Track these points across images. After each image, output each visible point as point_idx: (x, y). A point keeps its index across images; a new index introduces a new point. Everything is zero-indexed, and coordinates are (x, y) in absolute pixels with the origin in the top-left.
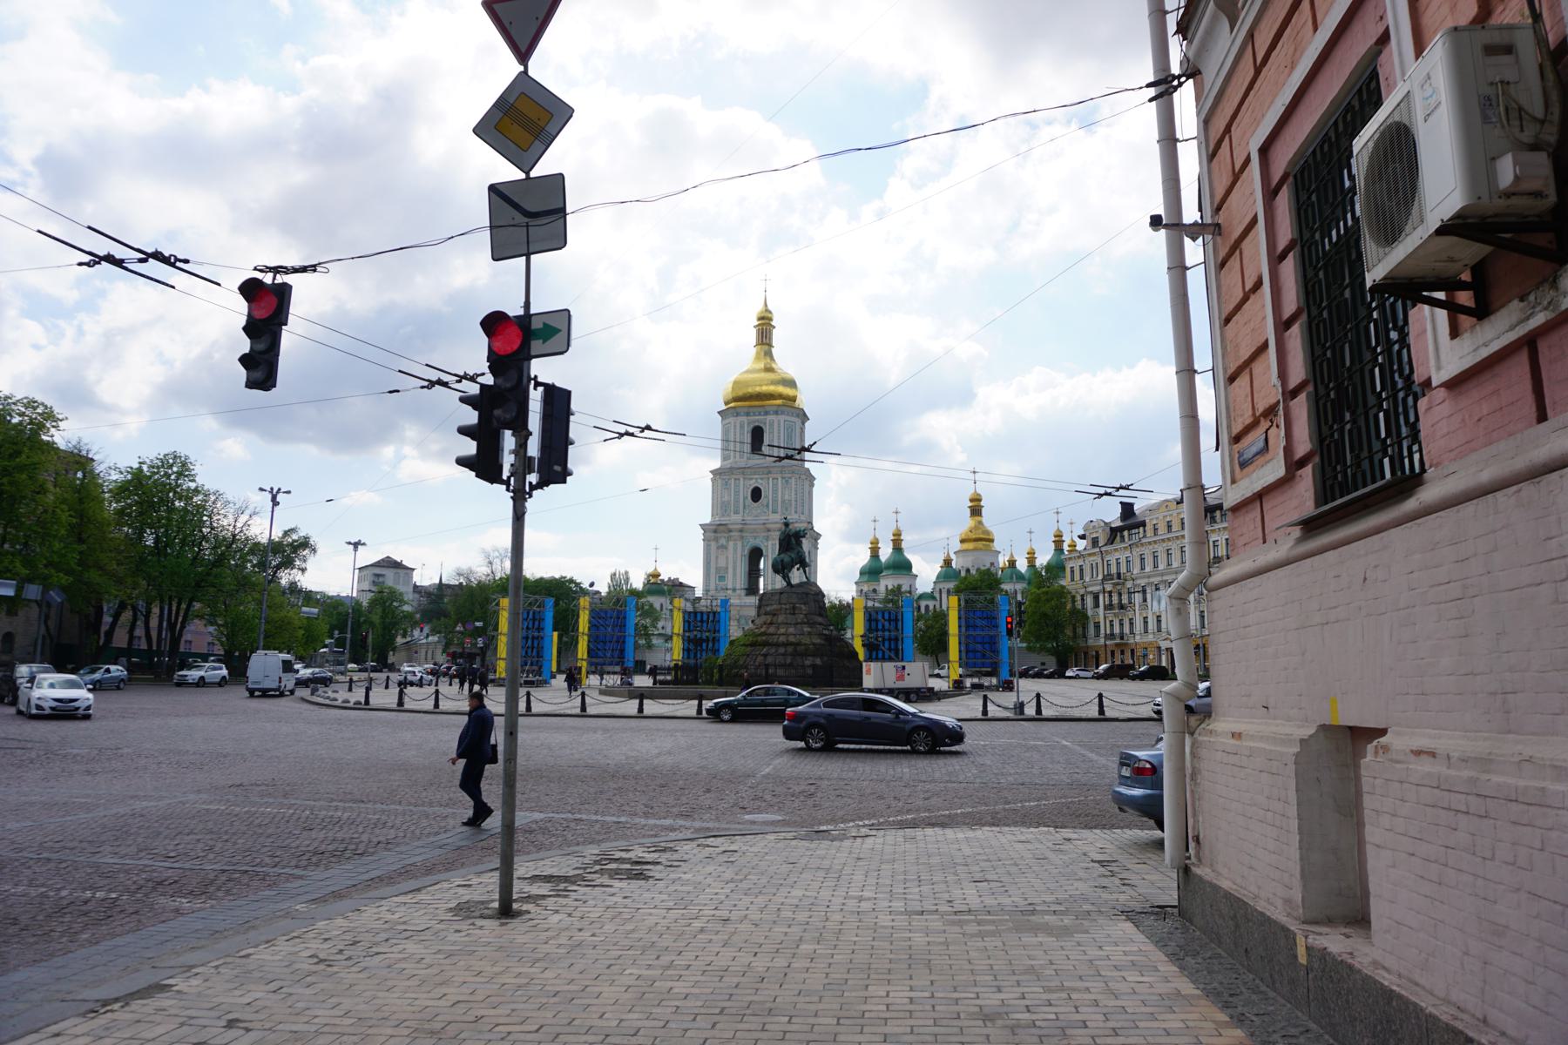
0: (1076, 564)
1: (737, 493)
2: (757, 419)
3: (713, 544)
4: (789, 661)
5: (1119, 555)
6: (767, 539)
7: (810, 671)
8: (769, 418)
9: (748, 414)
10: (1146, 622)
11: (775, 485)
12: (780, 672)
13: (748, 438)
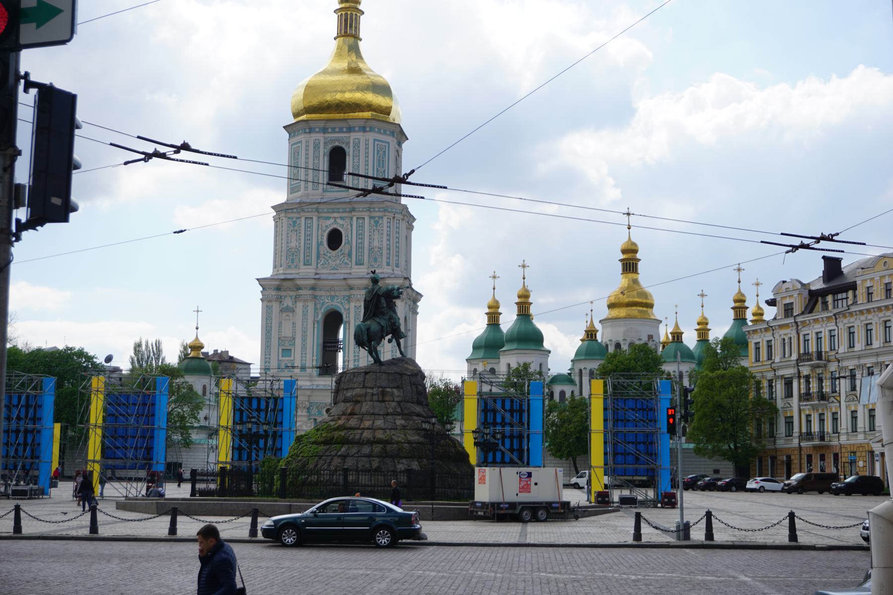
0: (762, 339)
1: (308, 237)
2: (337, 138)
3: (276, 306)
4: (375, 464)
5: (820, 328)
6: (349, 299)
7: (403, 479)
8: (353, 135)
9: (324, 130)
10: (854, 418)
11: (361, 227)
12: (364, 479)
13: (324, 163)
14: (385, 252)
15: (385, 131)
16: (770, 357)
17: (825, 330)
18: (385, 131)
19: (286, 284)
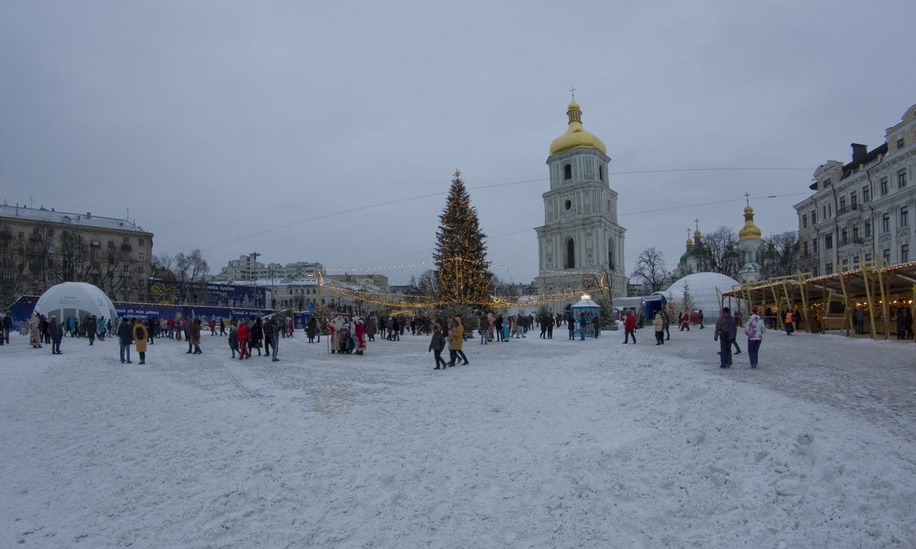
1: (556, 206)
3: (544, 240)
6: (575, 231)
8: (573, 157)
9: (560, 159)
11: (579, 197)
16: (814, 221)
17: (858, 188)
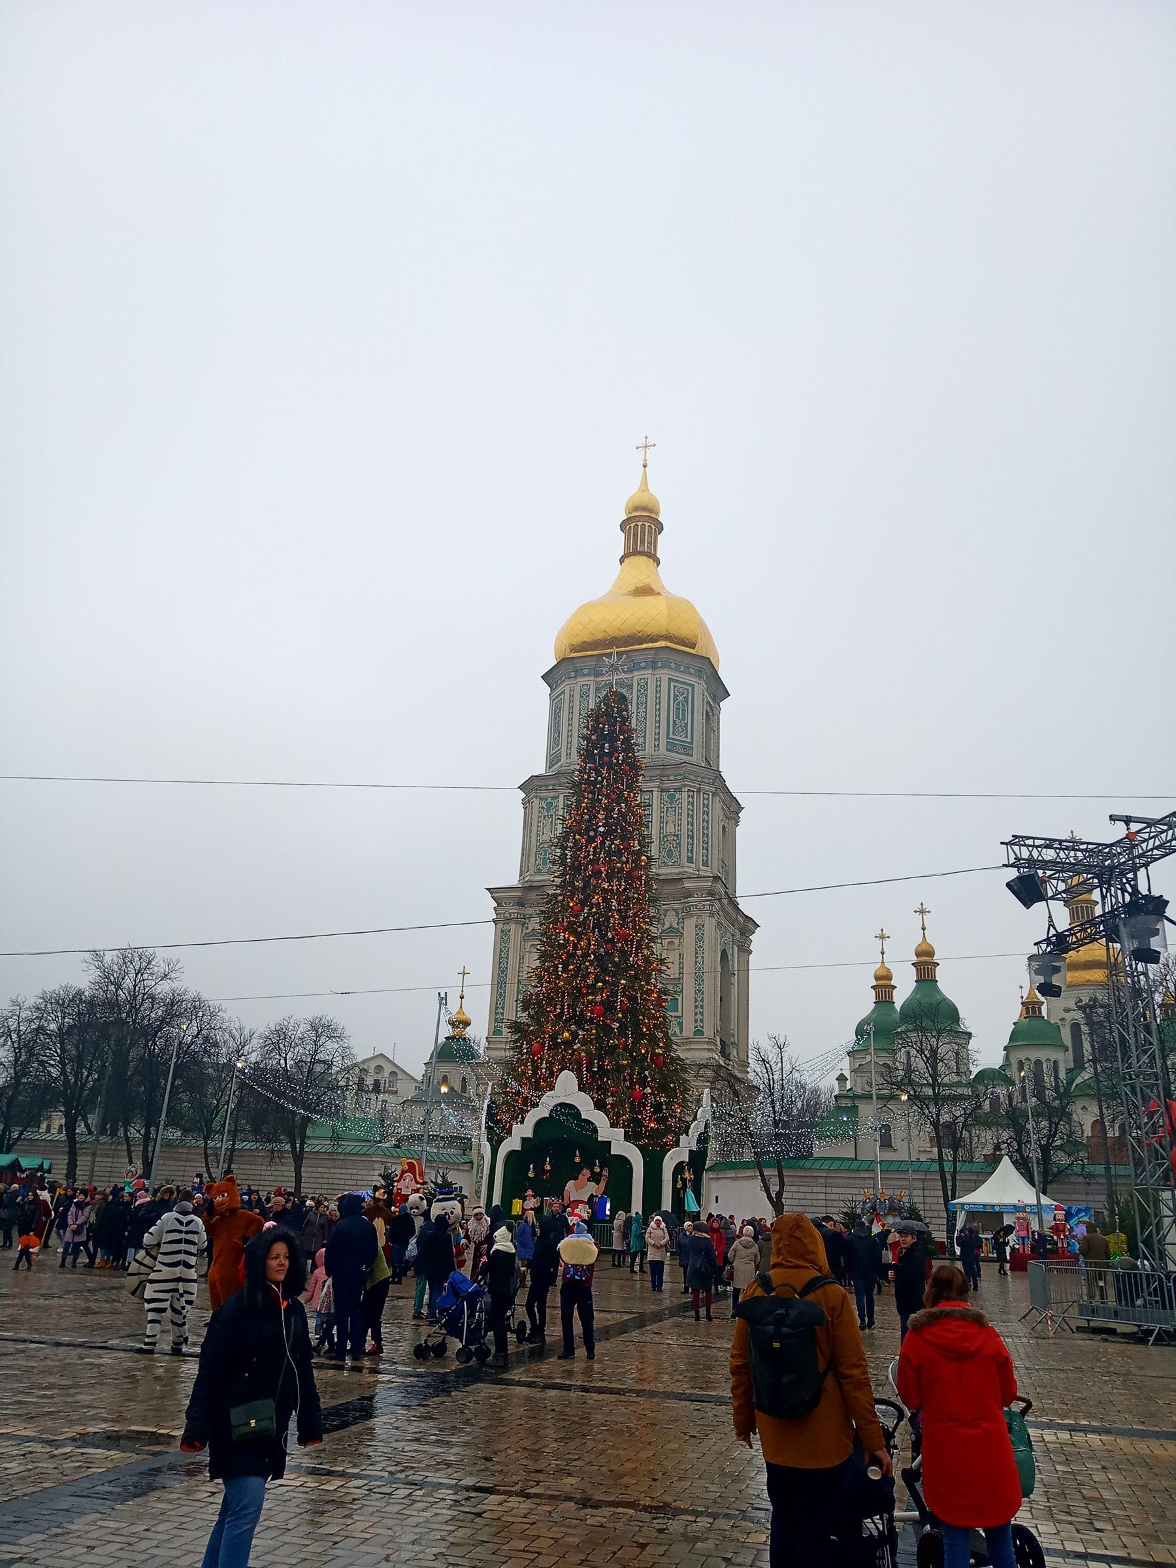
9: (597, 673)
14: (684, 841)
15: (687, 668)
18: (687, 668)
19: (532, 896)
